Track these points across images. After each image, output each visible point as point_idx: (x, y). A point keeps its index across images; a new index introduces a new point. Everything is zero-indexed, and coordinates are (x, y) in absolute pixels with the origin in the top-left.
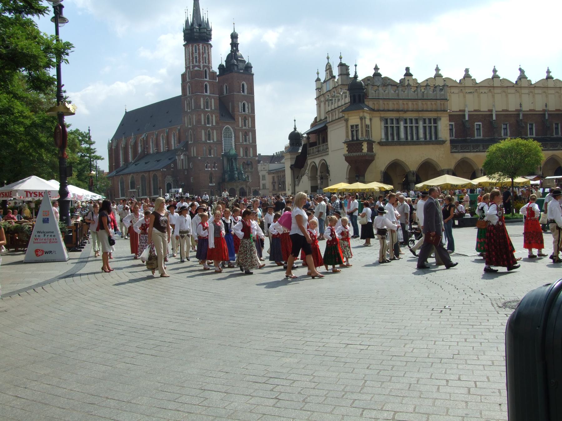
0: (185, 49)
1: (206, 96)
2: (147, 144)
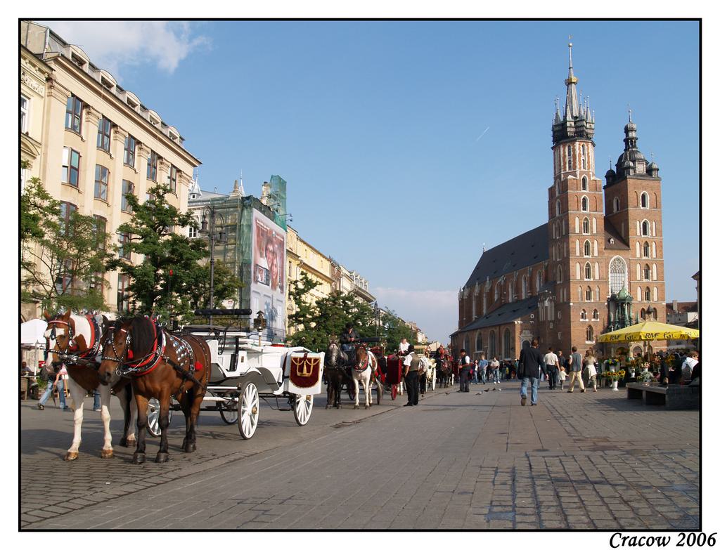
0: (554, 153)
1: (584, 214)
2: (504, 291)
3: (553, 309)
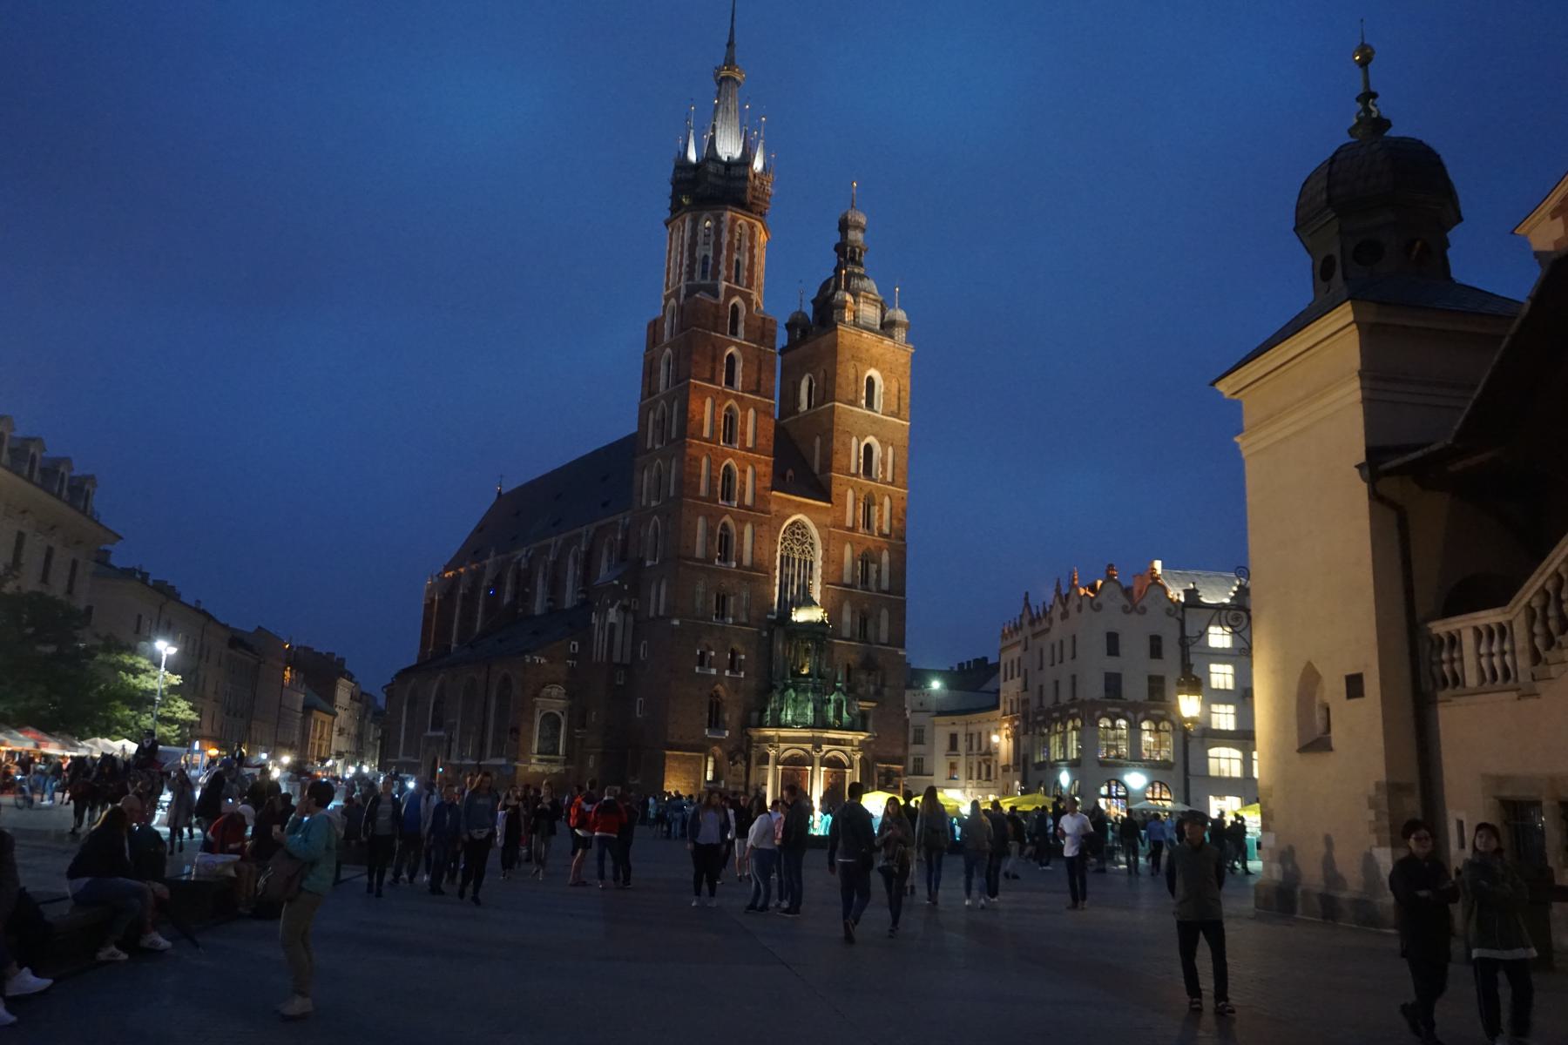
0: (671, 235)
1: (728, 396)
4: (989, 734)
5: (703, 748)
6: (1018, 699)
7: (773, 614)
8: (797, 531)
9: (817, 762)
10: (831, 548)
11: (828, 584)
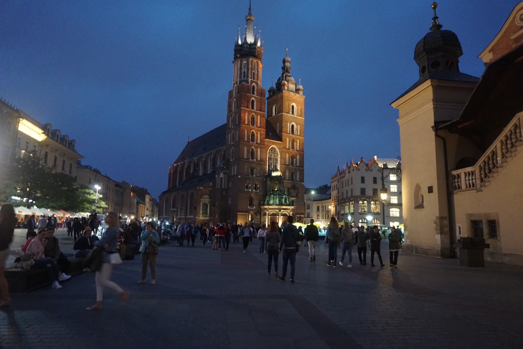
0: (234, 66)
3: (226, 180)
4: (328, 206)
5: (248, 211)
6: (336, 196)
7: (266, 173)
8: (273, 150)
9: (280, 215)
10: (282, 155)
11: (282, 165)
